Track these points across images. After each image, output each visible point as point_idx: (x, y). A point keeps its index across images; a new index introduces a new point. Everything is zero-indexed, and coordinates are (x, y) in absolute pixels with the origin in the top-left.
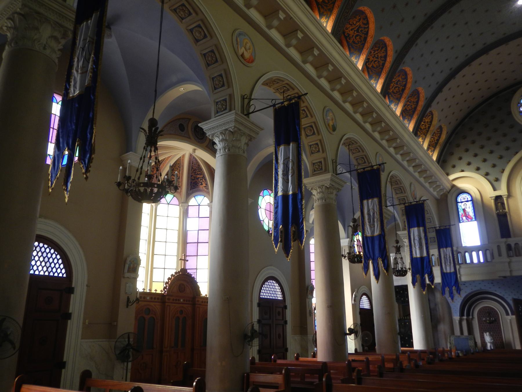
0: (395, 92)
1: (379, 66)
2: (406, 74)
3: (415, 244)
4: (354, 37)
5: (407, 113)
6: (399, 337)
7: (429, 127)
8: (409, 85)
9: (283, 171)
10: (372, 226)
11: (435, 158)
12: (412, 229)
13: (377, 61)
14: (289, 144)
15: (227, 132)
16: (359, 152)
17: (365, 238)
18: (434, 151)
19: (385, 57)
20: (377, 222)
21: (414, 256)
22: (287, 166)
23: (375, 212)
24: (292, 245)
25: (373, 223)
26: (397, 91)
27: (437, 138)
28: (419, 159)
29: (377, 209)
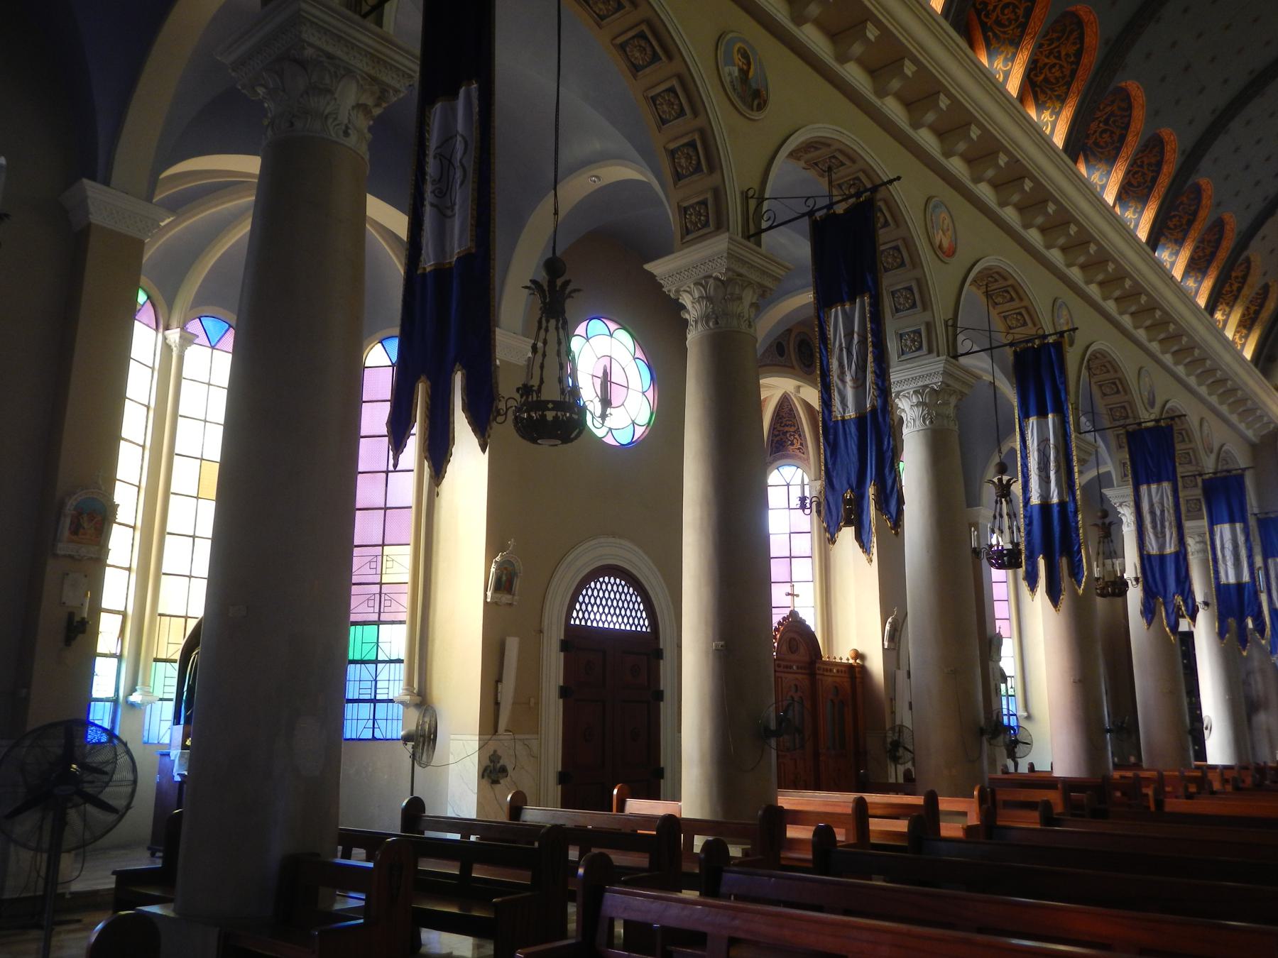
0: (1172, 226)
1: (1144, 183)
2: (1198, 191)
3: (1224, 556)
4: (1097, 134)
5: (1196, 266)
6: (1190, 738)
7: (1240, 290)
8: (1203, 213)
9: (1039, 463)
10: (1159, 536)
11: (1248, 354)
12: (1219, 526)
13: (1140, 174)
14: (1046, 416)
15: (928, 390)
16: (1108, 371)
17: (1145, 557)
18: (1246, 337)
19: (1159, 164)
20: (1170, 528)
21: (1223, 580)
22: (1044, 454)
23: (1165, 509)
24: (1063, 588)
25: (1161, 530)
26: (1175, 225)
27: (1257, 308)
28: (1221, 370)
29: (1169, 502)
